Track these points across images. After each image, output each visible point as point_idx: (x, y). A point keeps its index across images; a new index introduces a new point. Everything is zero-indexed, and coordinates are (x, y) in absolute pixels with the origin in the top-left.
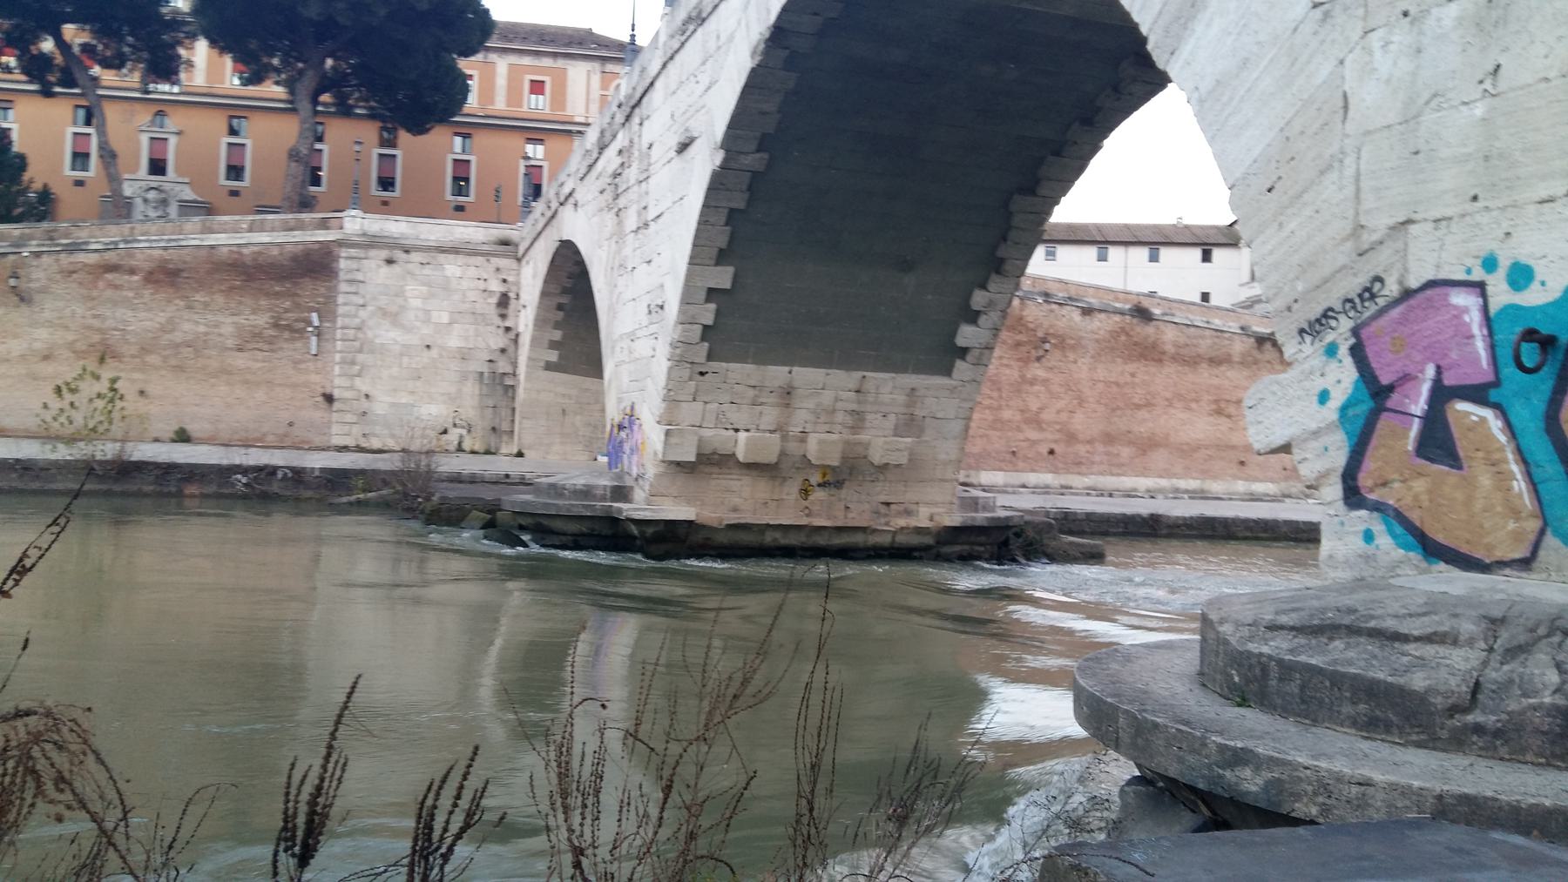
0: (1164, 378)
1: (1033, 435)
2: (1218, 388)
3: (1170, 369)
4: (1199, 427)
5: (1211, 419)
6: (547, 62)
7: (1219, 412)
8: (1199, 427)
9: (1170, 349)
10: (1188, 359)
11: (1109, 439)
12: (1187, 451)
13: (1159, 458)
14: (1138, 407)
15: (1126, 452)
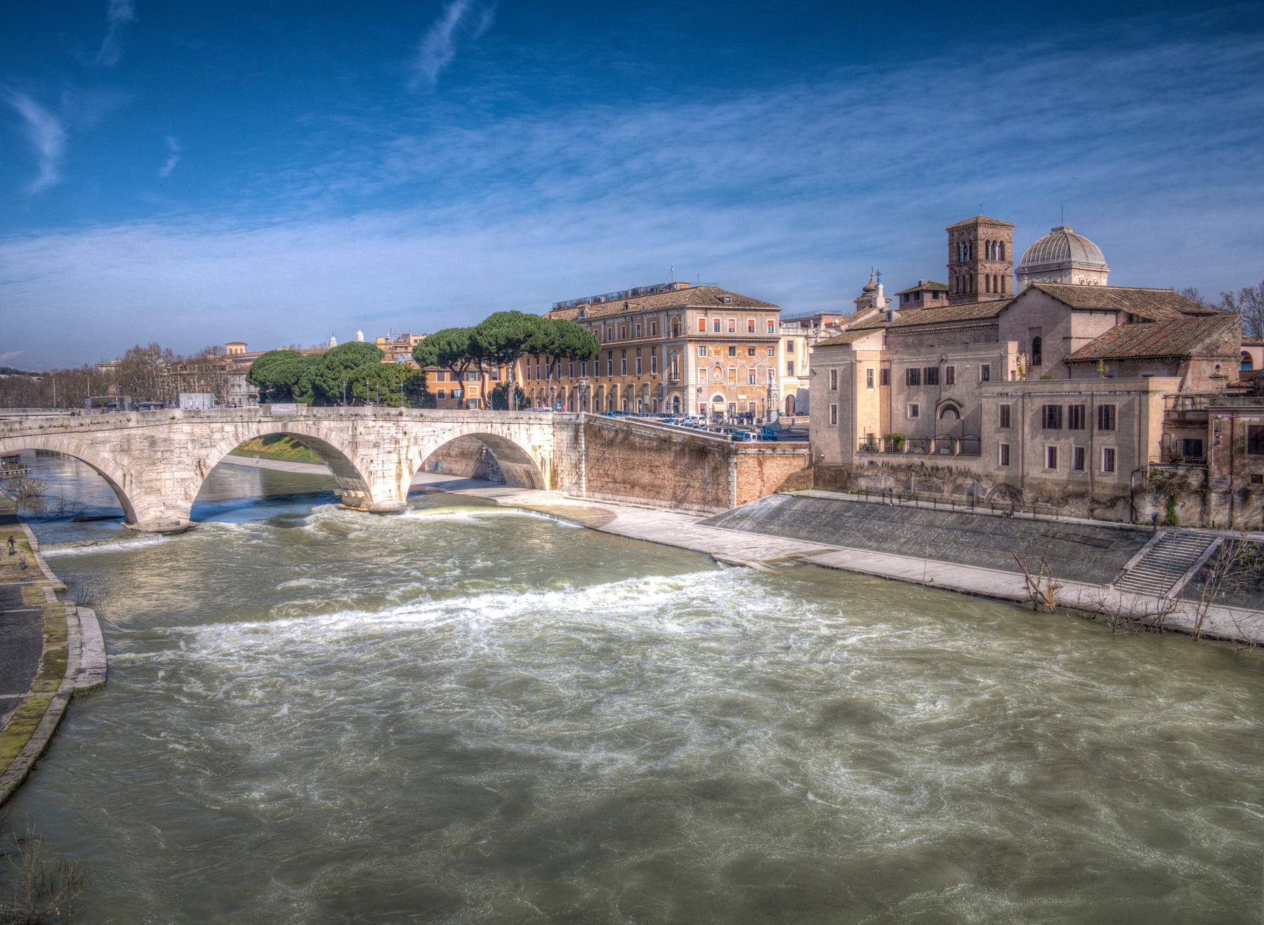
0: (637, 458)
1: (607, 480)
2: (651, 460)
3: (638, 453)
4: (646, 478)
5: (649, 474)
6: (655, 315)
7: (651, 471)
8: (646, 478)
9: (637, 444)
10: (643, 449)
11: (624, 482)
12: (643, 487)
13: (637, 488)
14: (631, 469)
15: (629, 487)
